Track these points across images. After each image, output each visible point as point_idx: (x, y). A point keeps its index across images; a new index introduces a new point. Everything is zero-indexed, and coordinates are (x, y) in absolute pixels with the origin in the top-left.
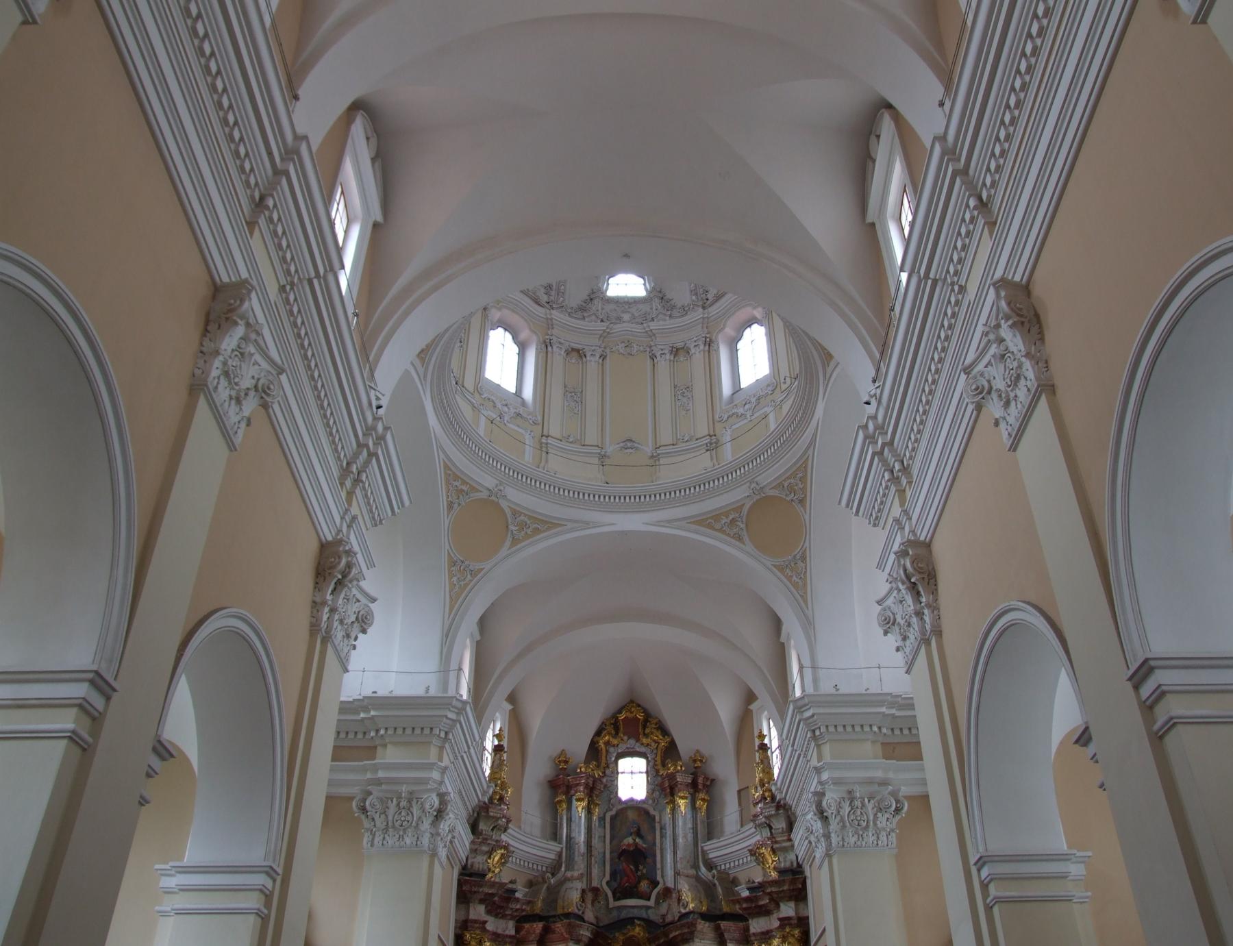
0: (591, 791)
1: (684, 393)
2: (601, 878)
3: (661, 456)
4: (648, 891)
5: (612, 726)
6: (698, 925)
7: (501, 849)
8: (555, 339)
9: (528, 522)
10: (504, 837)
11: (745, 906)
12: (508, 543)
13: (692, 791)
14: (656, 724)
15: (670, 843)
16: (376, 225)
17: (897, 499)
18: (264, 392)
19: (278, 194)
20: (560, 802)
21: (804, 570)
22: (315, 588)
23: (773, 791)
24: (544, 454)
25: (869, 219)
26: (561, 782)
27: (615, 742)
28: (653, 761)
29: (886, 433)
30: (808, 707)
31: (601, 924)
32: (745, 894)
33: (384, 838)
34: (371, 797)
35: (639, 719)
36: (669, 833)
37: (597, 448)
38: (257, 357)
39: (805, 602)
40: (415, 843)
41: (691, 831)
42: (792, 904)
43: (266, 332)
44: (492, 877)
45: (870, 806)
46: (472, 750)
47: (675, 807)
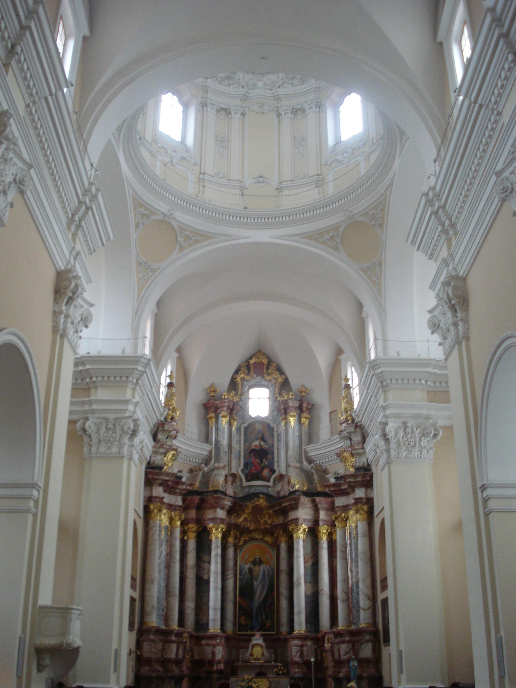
0: (231, 410)
1: (300, 143)
2: (237, 467)
3: (283, 189)
4: (269, 476)
5: (246, 368)
7: (173, 450)
8: (208, 100)
9: (191, 236)
10: (174, 442)
11: (332, 489)
12: (177, 251)
13: (299, 412)
14: (276, 367)
15: (284, 445)
16: (85, 38)
17: (445, 245)
18: (20, 183)
19: (24, 43)
20: (211, 418)
21: (380, 273)
22: (54, 302)
23: (353, 415)
24: (202, 188)
25: (440, 38)
27: (248, 378)
29: (441, 200)
30: (379, 366)
31: (238, 497)
32: (332, 481)
35: (264, 364)
36: (283, 438)
37: (238, 182)
38: (15, 160)
39: (380, 294)
41: (298, 438)
42: (363, 489)
43: (20, 143)
44: (166, 469)
45: (417, 432)
46: (154, 389)
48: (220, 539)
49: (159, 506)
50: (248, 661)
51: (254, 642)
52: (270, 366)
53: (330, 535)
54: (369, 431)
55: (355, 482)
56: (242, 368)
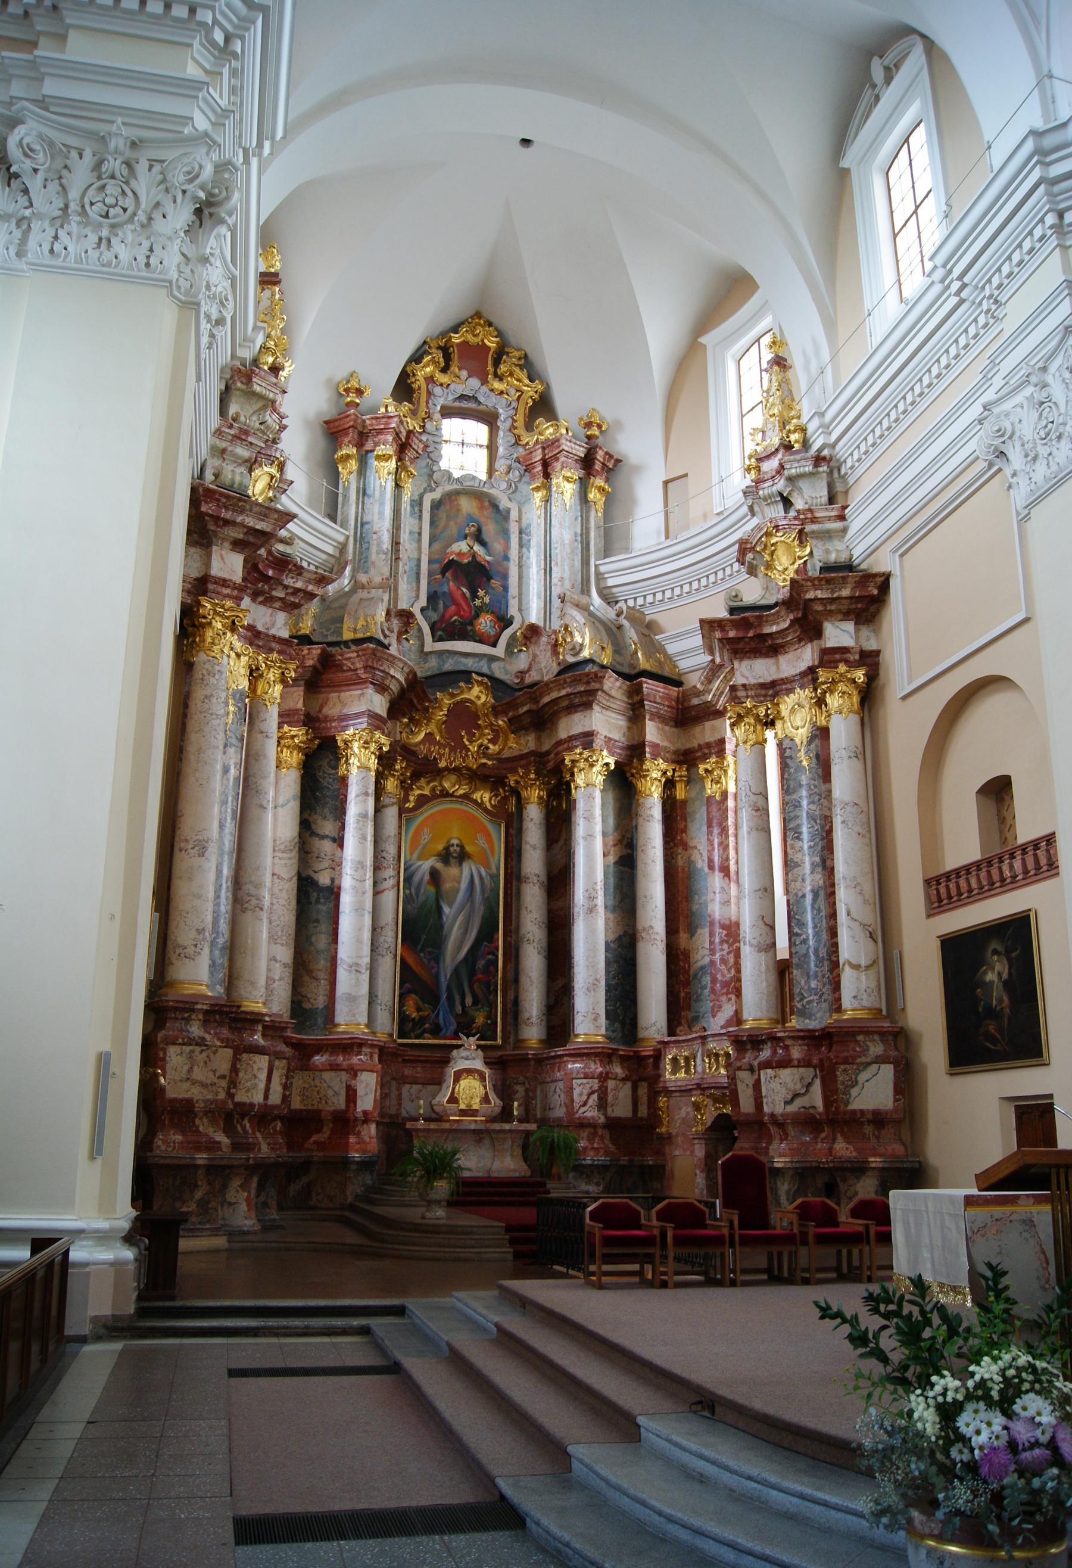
0: (403, 447)
6: (605, 681)
11: (732, 634)
14: (520, 359)
20: (348, 457)
26: (351, 423)
28: (510, 420)
33: (56, 238)
34: (20, 131)
35: (489, 348)
40: (142, 260)
42: (850, 626)
47: (551, 496)
48: (373, 773)
49: (231, 609)
50: (439, 1118)
51: (460, 1064)
52: (505, 357)
53: (669, 785)
54: (859, 472)
55: (833, 600)
56: (434, 350)
